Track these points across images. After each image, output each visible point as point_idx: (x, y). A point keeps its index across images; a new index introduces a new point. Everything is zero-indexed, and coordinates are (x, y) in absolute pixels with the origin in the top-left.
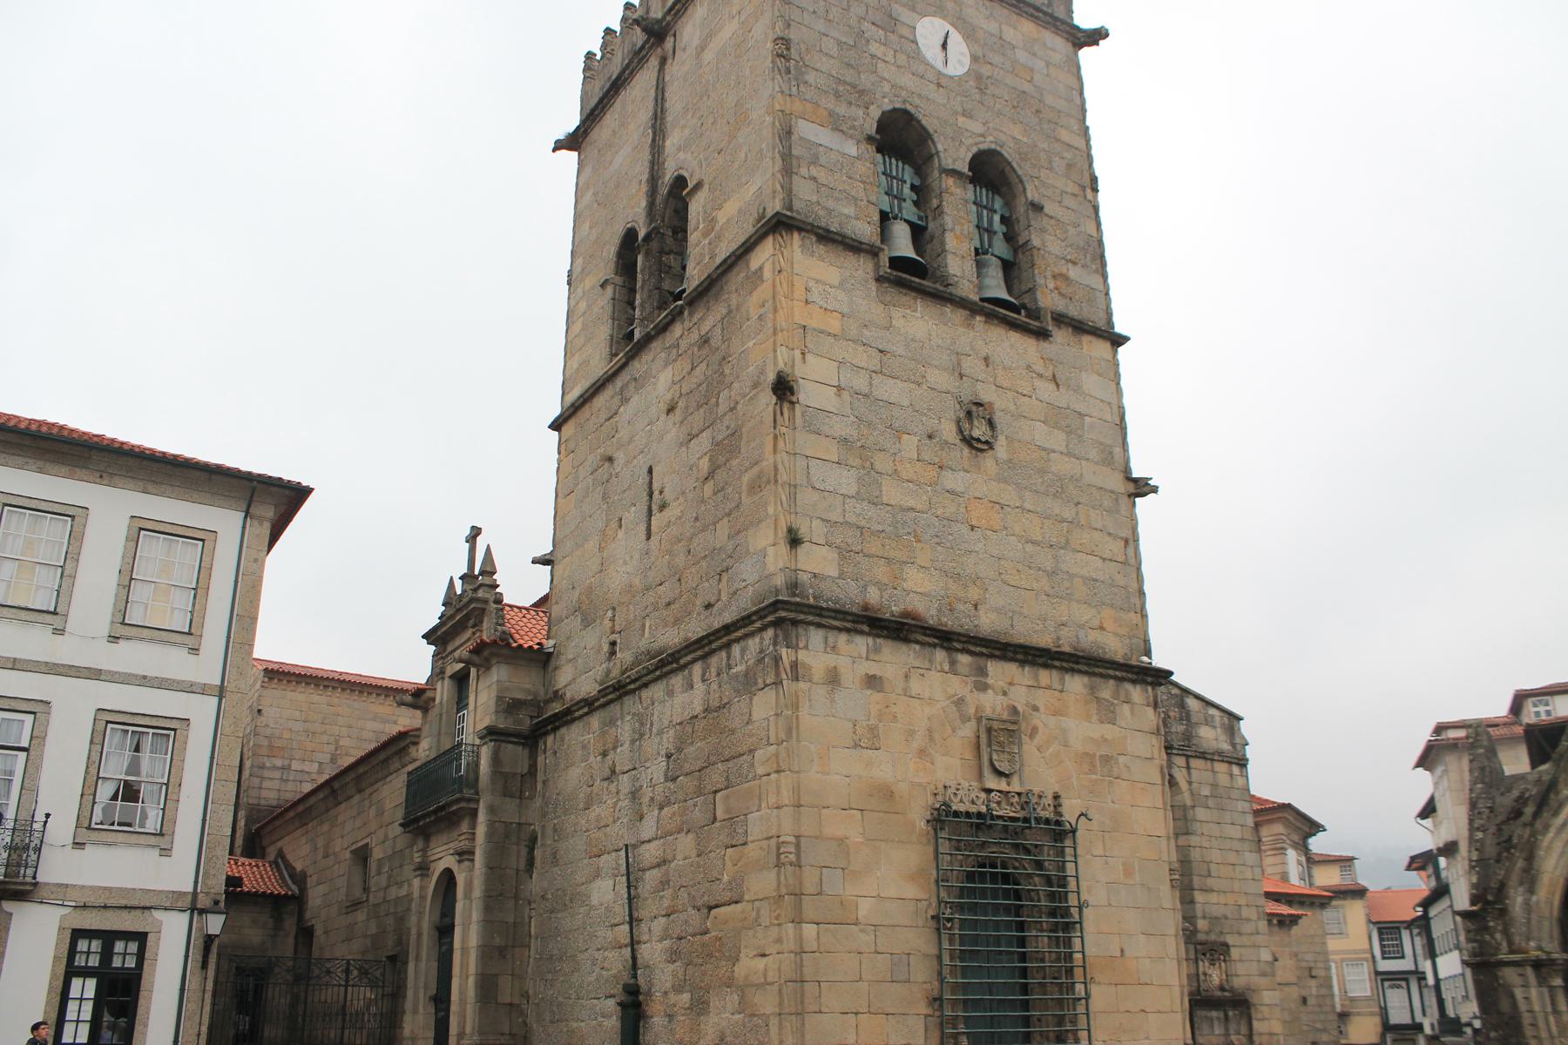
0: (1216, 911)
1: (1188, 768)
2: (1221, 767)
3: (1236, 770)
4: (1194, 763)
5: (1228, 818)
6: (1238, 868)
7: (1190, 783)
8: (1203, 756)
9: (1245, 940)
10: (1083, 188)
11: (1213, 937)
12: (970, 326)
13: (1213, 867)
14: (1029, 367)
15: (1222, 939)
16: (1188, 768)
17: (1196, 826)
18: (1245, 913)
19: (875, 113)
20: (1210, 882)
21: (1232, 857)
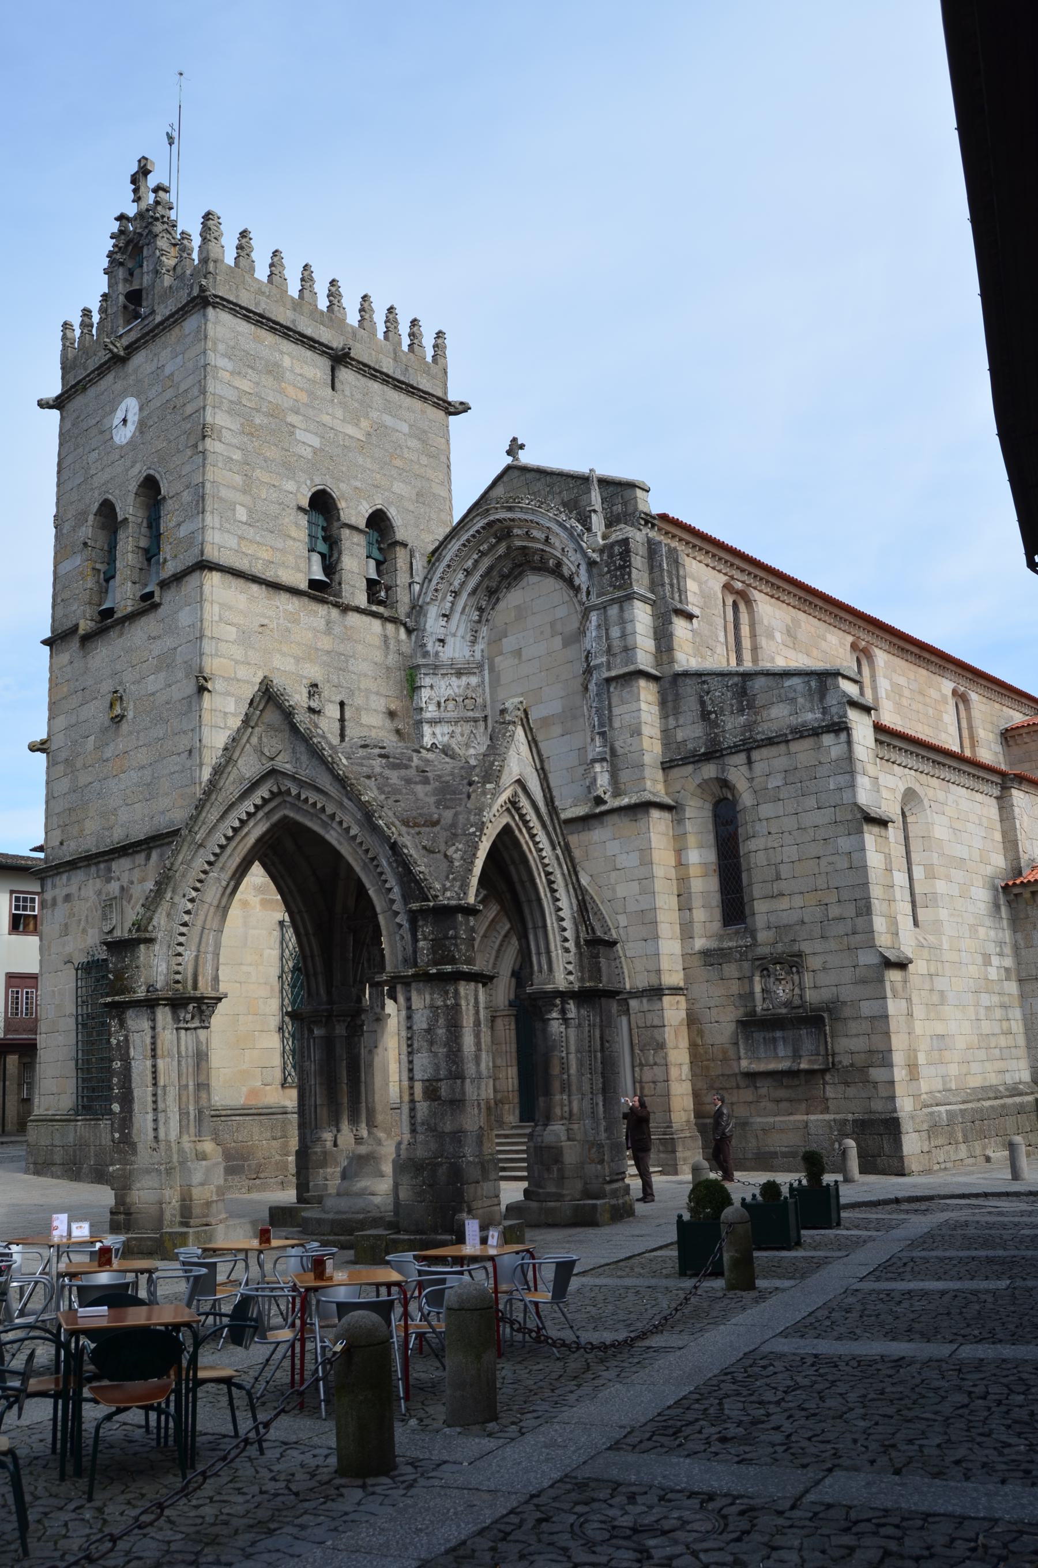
0: (787, 918)
1: (750, 762)
2: (802, 749)
3: (828, 739)
4: (756, 755)
5: (811, 802)
6: (823, 862)
7: (751, 780)
8: (770, 742)
9: (832, 945)
10: (196, 446)
11: (780, 948)
12: (121, 634)
13: (785, 870)
14: (150, 638)
15: (796, 948)
16: (750, 762)
17: (761, 828)
18: (834, 911)
19: (91, 517)
20: (777, 887)
21: (814, 850)
